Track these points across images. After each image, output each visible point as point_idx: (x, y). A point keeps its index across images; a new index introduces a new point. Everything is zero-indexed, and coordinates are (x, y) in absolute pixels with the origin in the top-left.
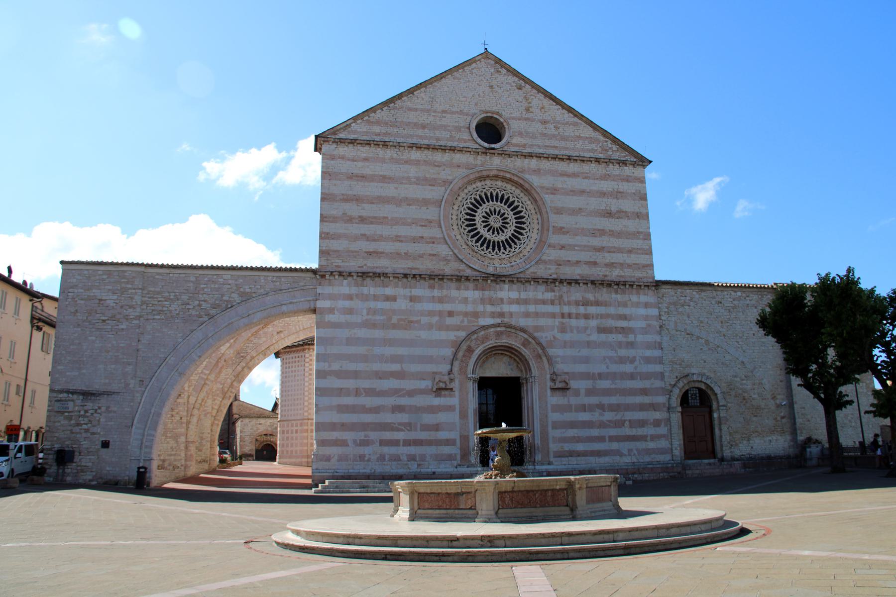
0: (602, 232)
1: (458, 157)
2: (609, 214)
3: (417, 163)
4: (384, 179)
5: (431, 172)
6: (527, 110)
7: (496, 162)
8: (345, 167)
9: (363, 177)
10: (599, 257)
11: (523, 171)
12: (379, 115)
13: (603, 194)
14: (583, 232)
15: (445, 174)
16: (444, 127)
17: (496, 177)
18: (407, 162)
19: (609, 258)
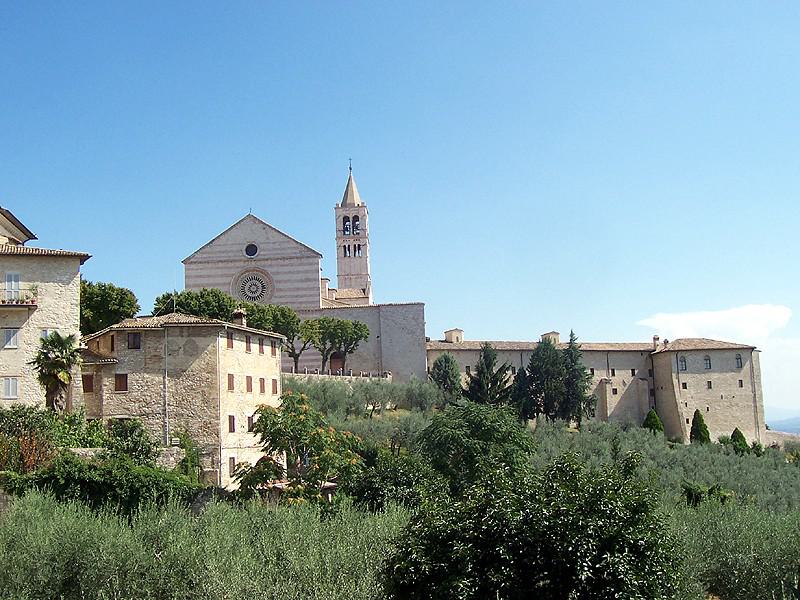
0: (298, 289)
1: (237, 264)
2: (302, 281)
3: (221, 268)
4: (209, 276)
5: (226, 272)
6: (268, 238)
7: (253, 263)
8: (194, 273)
9: (201, 276)
10: (294, 300)
11: (264, 266)
12: (204, 250)
13: (298, 272)
14: (290, 290)
15: (232, 272)
16: (232, 251)
17: (254, 270)
18: (218, 268)
19: (301, 300)
